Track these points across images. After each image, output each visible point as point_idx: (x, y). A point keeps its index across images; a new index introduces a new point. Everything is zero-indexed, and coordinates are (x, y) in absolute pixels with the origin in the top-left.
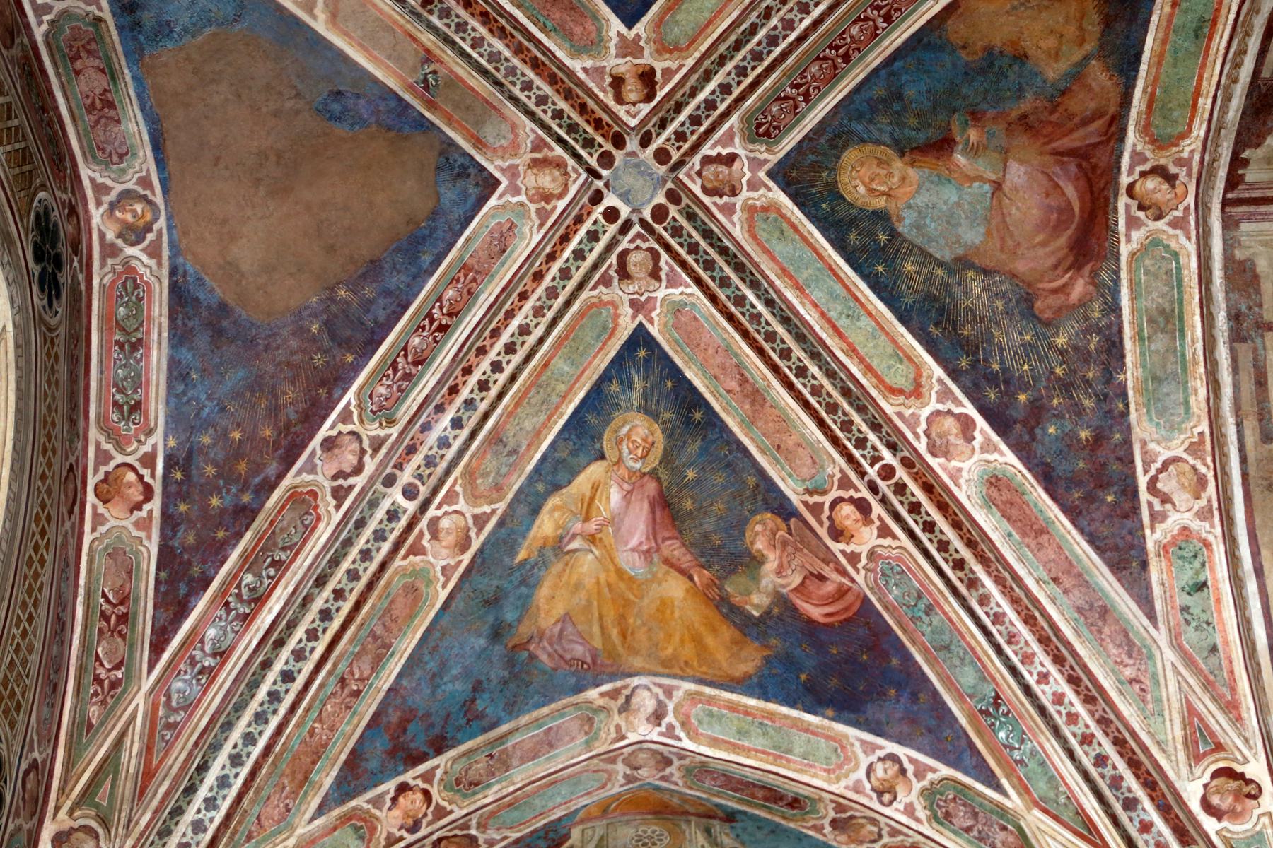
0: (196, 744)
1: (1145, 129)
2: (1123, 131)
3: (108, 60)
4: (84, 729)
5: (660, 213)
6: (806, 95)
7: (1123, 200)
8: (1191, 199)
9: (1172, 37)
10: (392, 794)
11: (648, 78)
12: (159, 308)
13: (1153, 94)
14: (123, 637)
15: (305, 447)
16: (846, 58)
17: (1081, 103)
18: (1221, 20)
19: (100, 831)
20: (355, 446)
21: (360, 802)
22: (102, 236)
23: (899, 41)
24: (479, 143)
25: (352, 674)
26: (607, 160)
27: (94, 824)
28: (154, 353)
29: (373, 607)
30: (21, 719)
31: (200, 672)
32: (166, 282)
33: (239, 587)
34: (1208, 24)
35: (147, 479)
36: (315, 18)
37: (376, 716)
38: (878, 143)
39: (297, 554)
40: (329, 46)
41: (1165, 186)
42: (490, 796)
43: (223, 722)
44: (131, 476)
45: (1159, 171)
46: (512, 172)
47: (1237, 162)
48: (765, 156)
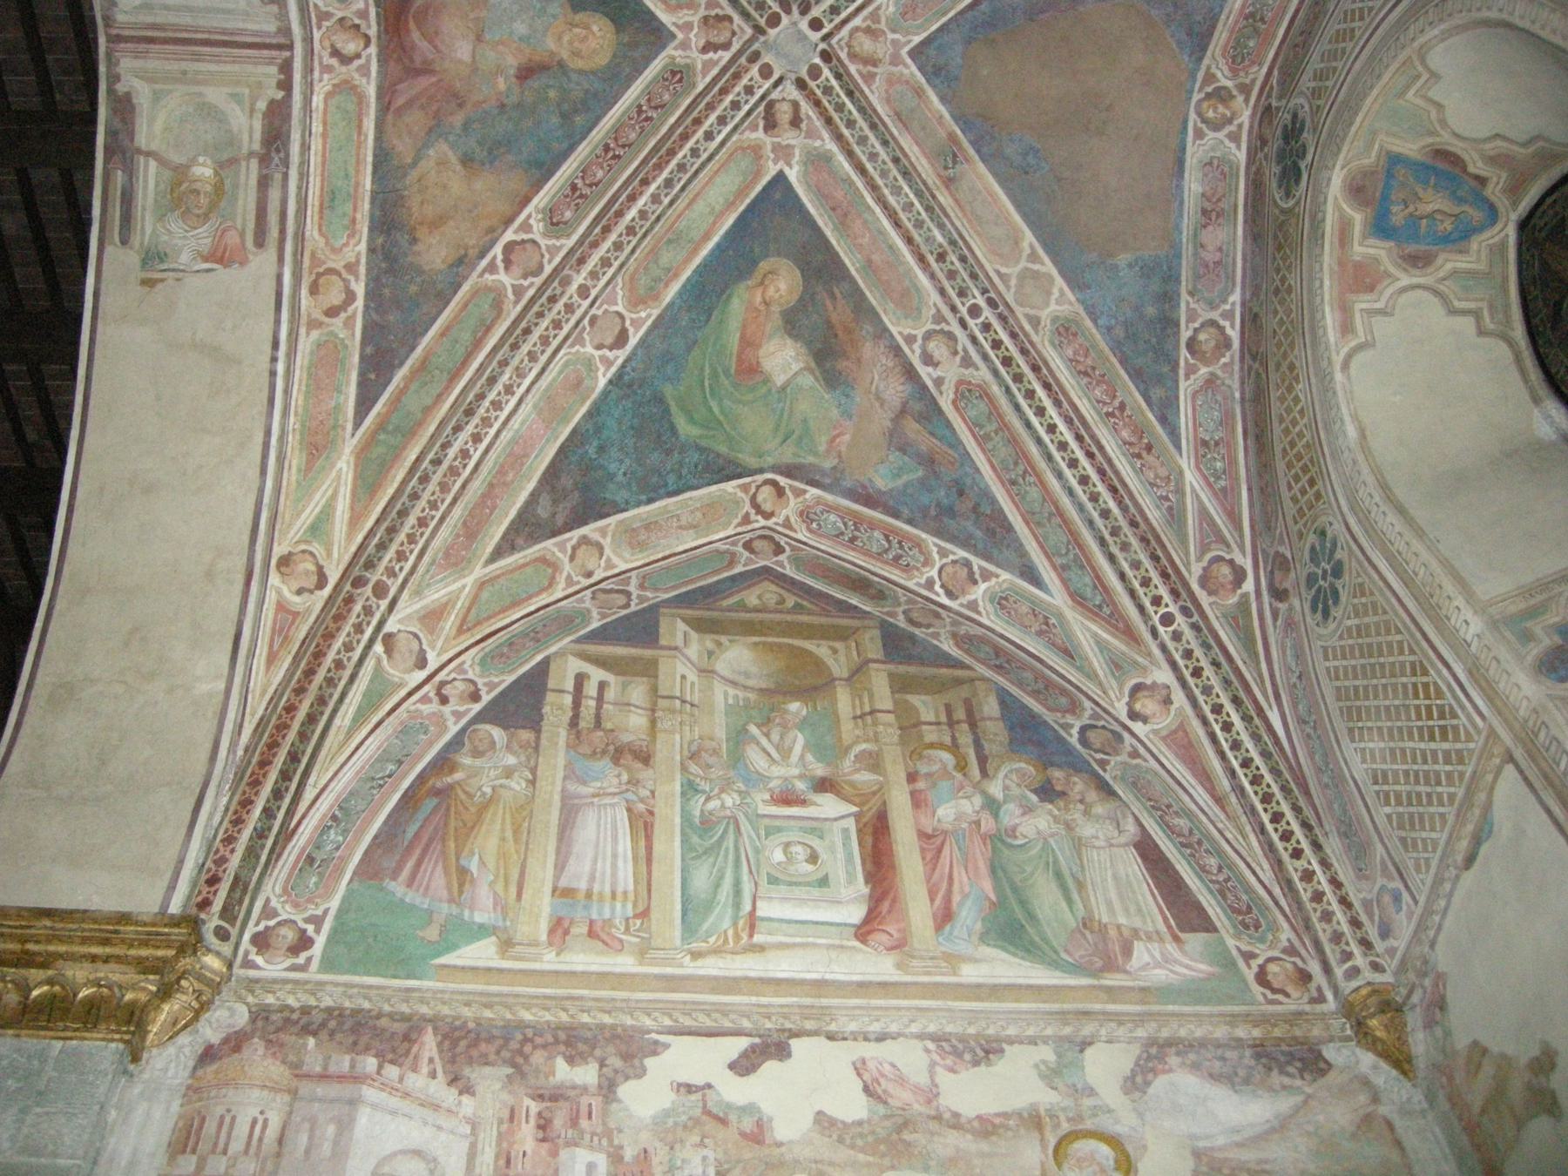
1: (361, 99)
2: (379, 97)
3: (1195, 254)
5: (774, 21)
6: (640, 111)
7: (373, 31)
8: (317, 35)
9: (352, 190)
11: (771, 125)
12: (1221, 36)
13: (359, 133)
16: (607, 148)
17: (416, 119)
18: (316, 209)
22: (1247, 100)
23: (564, 168)
24: (919, 92)
26: (815, 72)
32: (1209, 53)
34: (326, 205)
36: (1032, 246)
38: (581, 72)
40: (1025, 217)
41: (338, 46)
45: (346, 60)
46: (896, 60)
47: (286, 85)
48: (676, 53)
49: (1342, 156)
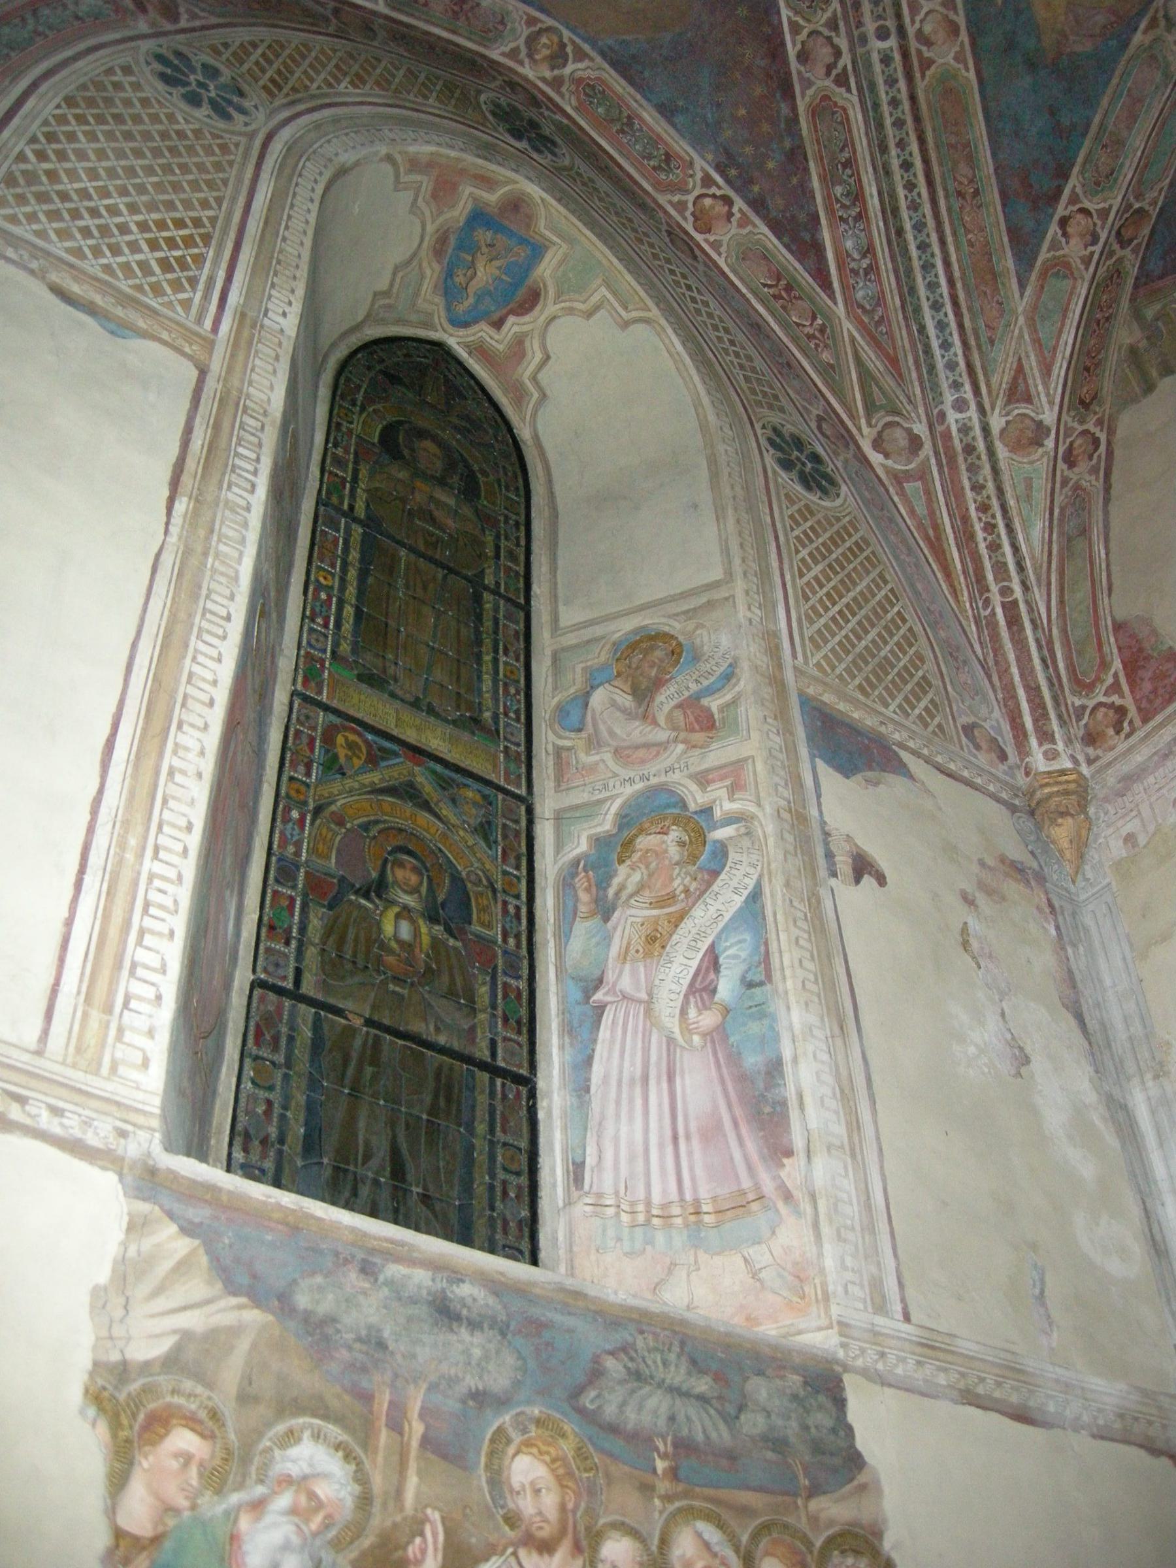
0: (905, 318)
4: (829, 371)
10: (1060, 232)
12: (619, 85)
14: (800, 298)
15: (788, 73)
19: (897, 419)
20: (821, 40)
21: (1044, 255)
22: (544, 80)
25: (961, 183)
27: (889, 419)
28: (645, 115)
29: (934, 130)
30: (784, 402)
31: (866, 274)
32: (606, 66)
33: (838, 201)
35: (718, 193)
37: (1004, 195)
39: (853, 145)
42: (1127, 173)
43: (908, 291)
44: (708, 202)
49: (554, 202)
